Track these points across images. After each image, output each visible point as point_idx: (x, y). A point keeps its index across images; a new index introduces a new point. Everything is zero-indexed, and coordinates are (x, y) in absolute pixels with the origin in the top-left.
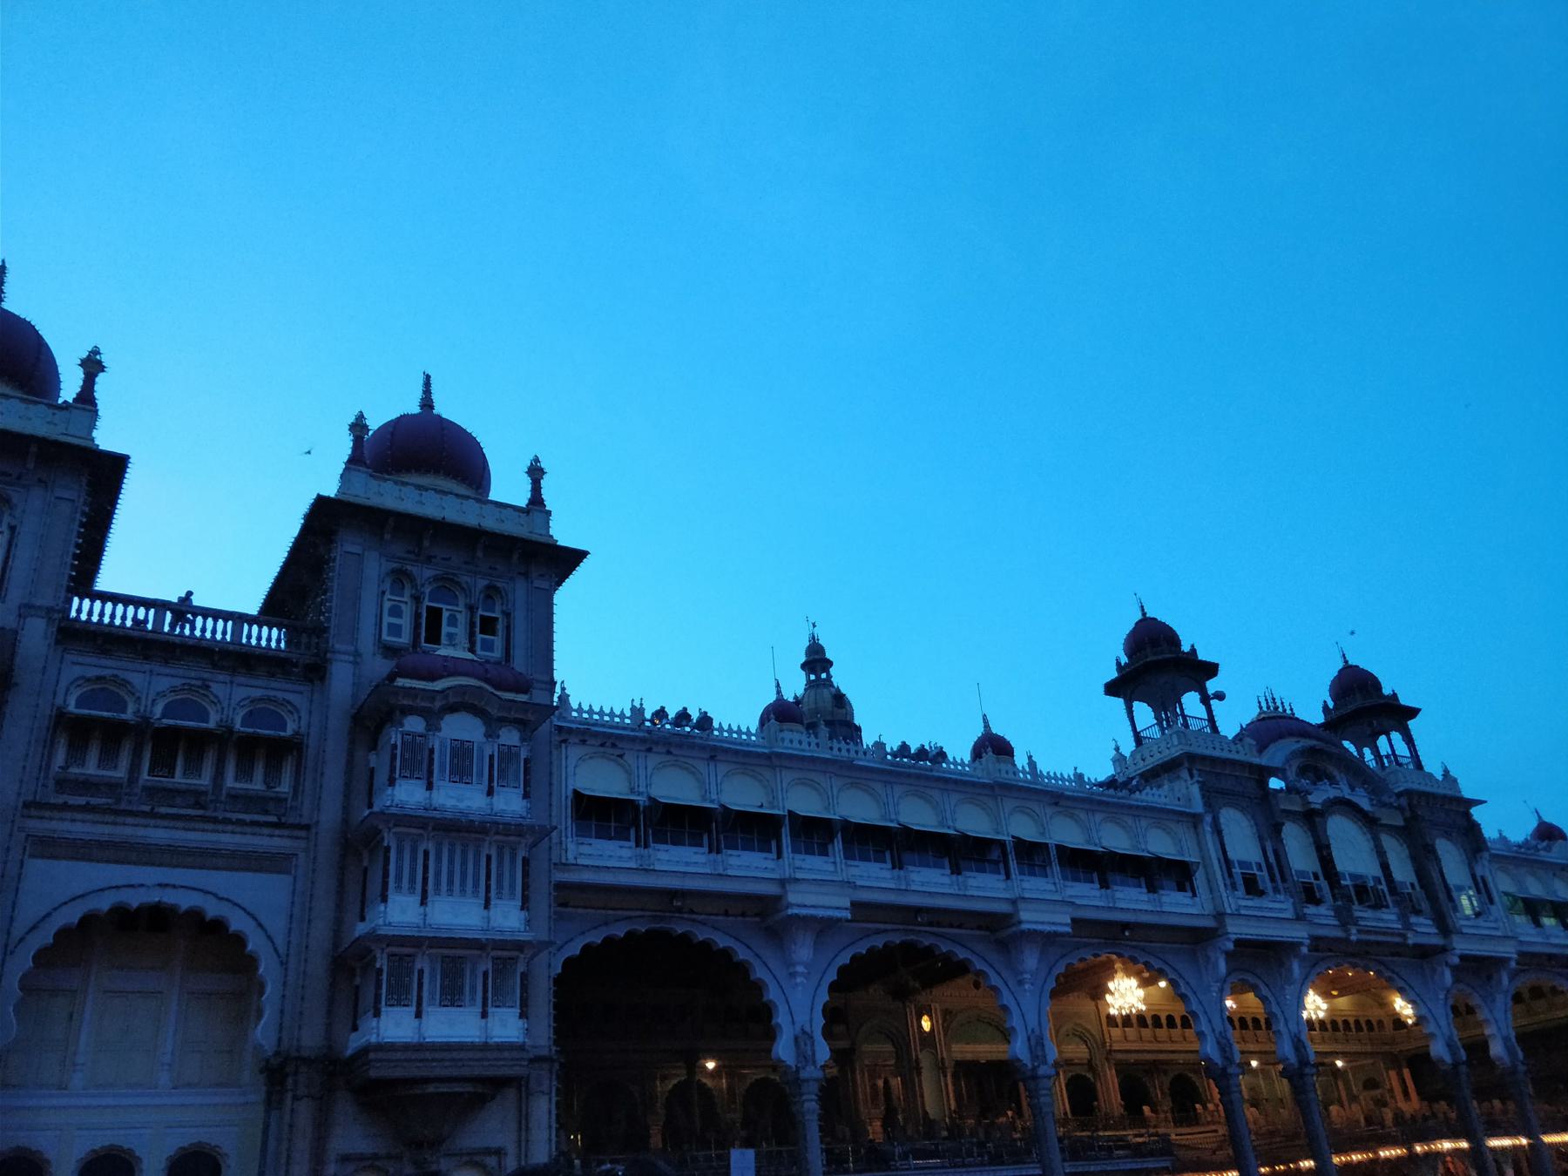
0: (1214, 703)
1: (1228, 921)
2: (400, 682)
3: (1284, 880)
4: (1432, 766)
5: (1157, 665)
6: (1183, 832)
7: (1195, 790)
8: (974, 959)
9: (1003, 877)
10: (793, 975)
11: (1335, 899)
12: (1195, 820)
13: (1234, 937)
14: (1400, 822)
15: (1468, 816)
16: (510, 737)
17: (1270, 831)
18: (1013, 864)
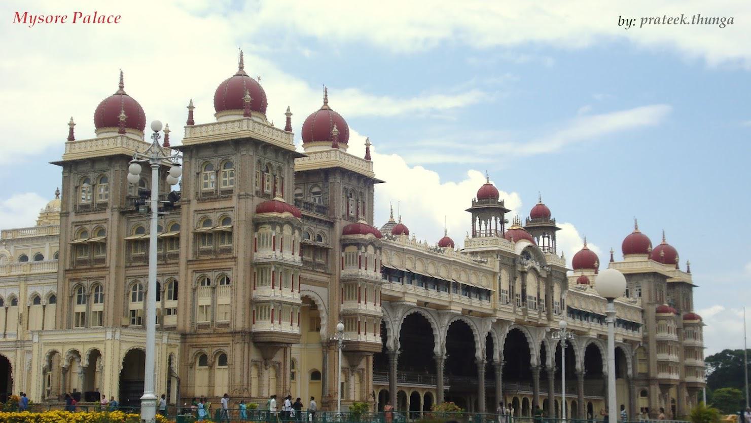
0: (505, 224)
1: (498, 312)
2: (361, 236)
3: (513, 298)
4: (559, 254)
5: (487, 205)
6: (490, 277)
7: (498, 264)
8: (432, 319)
9: (448, 293)
10: (395, 321)
11: (523, 305)
12: (494, 274)
13: (497, 318)
14: (544, 275)
15: (565, 275)
16: (378, 251)
17: (513, 279)
18: (451, 289)
